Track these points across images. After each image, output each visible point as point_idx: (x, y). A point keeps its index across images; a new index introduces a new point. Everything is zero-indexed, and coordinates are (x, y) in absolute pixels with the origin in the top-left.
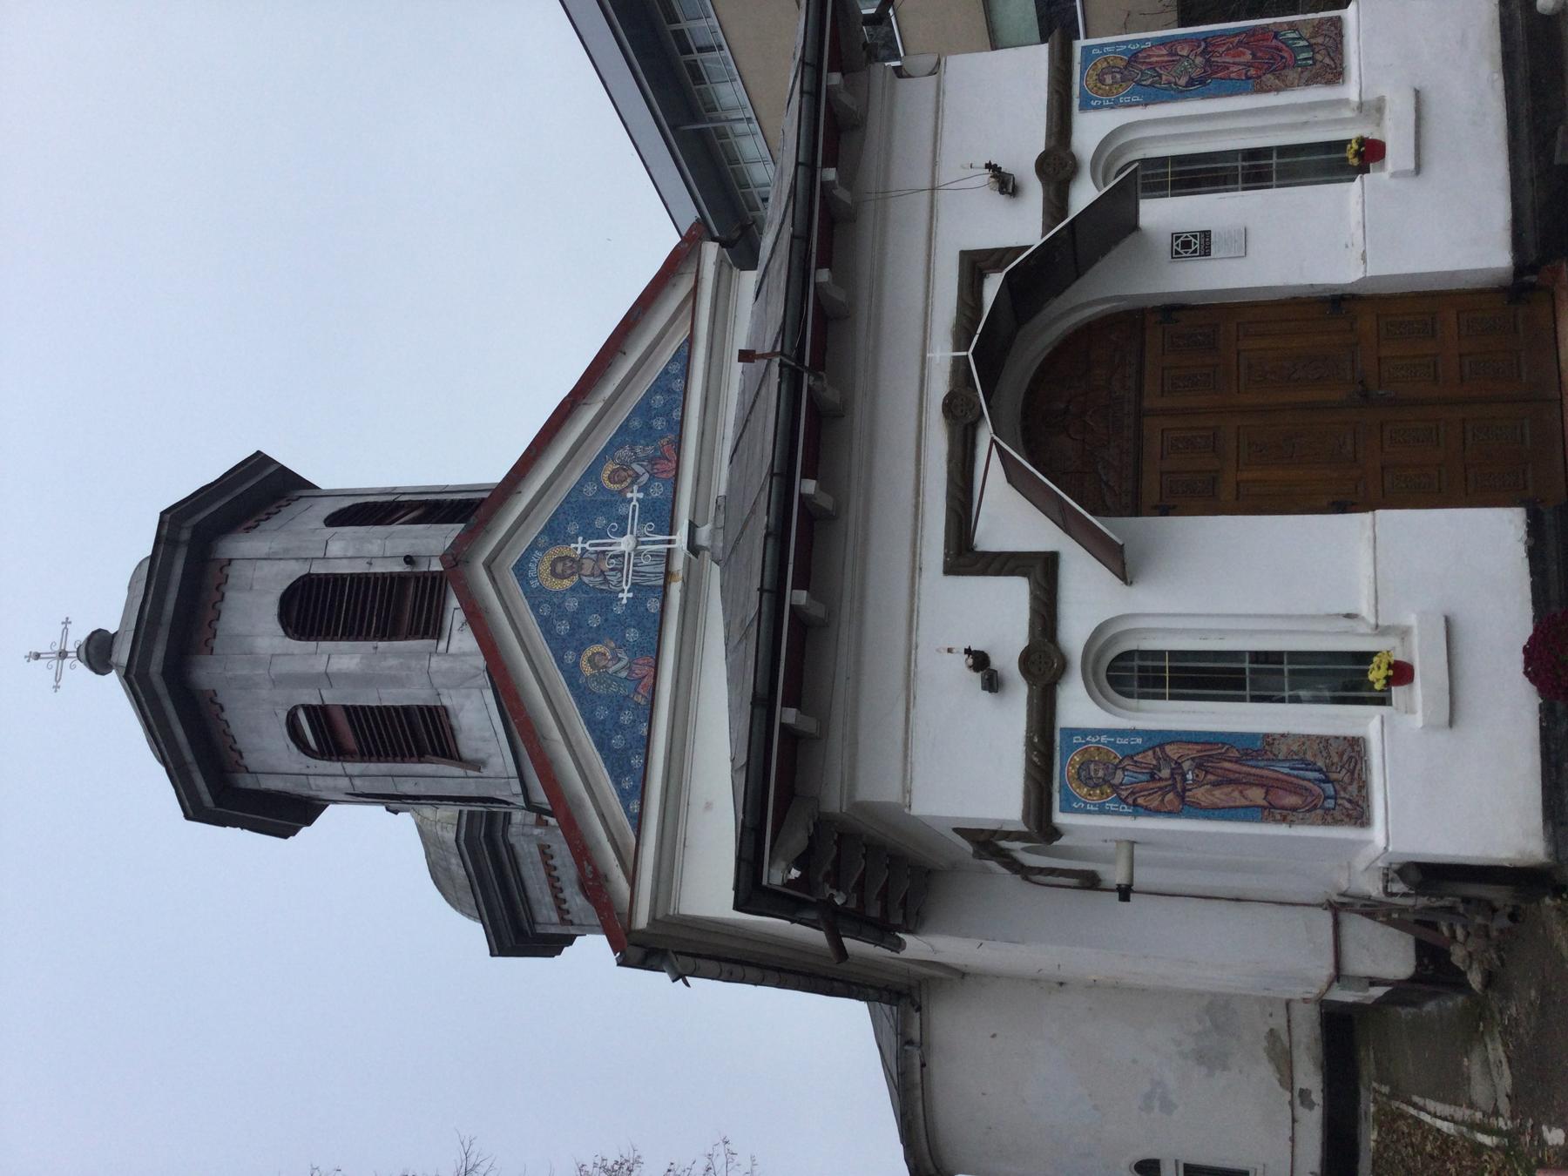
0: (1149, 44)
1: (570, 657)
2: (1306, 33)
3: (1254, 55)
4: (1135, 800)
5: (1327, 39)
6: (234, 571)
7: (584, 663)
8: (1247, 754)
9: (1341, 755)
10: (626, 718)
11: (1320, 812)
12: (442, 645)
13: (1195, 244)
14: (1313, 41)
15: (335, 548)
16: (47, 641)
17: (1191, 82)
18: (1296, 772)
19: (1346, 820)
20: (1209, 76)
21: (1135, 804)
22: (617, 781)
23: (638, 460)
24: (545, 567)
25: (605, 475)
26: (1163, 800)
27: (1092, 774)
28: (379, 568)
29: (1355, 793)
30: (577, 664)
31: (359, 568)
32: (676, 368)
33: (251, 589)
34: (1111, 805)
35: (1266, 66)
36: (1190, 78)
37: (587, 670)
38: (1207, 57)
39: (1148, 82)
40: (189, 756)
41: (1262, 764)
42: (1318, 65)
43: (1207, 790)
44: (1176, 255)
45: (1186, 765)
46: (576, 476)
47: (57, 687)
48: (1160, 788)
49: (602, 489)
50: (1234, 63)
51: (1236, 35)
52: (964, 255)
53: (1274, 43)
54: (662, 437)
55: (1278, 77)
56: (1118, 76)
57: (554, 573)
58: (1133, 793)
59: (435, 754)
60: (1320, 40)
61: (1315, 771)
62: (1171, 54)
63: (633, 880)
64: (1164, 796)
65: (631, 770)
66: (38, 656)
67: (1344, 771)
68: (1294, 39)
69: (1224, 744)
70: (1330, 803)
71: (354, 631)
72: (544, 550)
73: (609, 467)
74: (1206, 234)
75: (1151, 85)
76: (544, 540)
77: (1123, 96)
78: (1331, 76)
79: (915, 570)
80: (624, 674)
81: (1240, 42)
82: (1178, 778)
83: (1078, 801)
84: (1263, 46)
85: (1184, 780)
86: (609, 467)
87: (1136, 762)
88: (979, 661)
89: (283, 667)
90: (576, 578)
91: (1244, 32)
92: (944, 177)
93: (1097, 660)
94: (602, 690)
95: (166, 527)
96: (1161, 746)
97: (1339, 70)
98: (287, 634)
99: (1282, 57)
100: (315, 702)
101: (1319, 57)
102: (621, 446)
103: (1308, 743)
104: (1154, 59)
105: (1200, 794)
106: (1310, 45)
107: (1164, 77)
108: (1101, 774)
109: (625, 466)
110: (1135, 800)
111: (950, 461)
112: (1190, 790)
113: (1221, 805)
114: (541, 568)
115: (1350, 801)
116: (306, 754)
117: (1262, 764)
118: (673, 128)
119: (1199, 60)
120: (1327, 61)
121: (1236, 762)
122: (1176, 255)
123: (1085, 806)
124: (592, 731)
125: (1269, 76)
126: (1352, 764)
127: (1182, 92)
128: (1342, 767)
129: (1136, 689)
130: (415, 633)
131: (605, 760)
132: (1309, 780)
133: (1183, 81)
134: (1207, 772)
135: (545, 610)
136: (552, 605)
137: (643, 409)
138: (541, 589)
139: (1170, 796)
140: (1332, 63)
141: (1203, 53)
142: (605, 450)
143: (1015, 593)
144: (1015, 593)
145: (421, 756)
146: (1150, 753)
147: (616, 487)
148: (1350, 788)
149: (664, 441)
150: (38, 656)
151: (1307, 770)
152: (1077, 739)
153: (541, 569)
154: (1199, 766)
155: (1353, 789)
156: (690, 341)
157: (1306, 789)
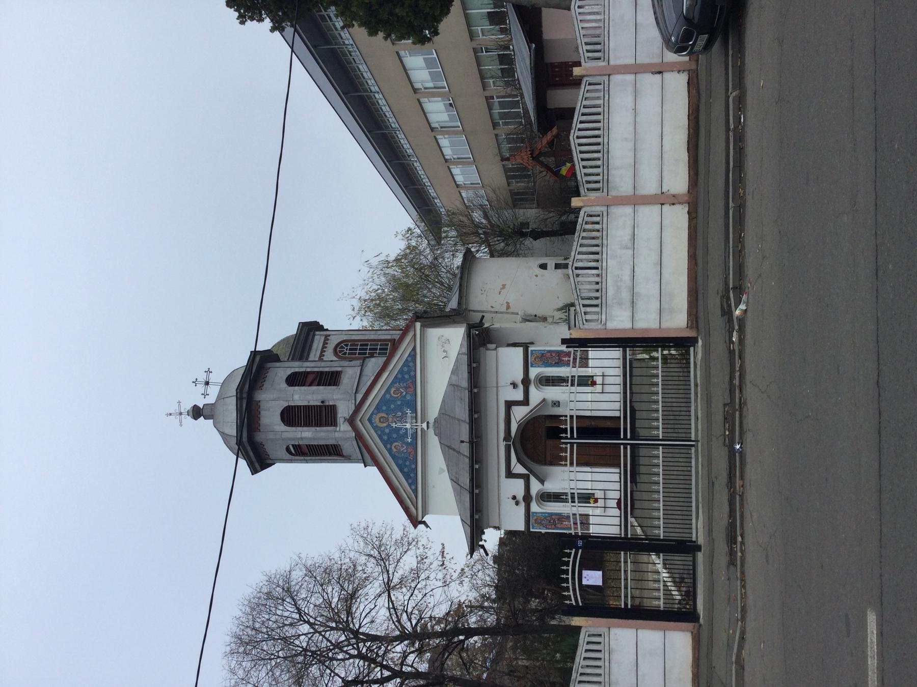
1: (389, 446)
6: (262, 404)
7: (393, 448)
10: (408, 463)
12: (338, 429)
15: (296, 397)
16: (174, 408)
17: (555, 363)
21: (546, 527)
22: (407, 480)
23: (402, 388)
24: (377, 420)
25: (392, 392)
28: (312, 403)
30: (391, 448)
31: (305, 403)
32: (409, 359)
33: (269, 411)
37: (395, 450)
40: (254, 459)
44: (553, 406)
45: (556, 520)
46: (383, 392)
47: (181, 425)
49: (391, 396)
52: (506, 402)
54: (408, 381)
57: (380, 421)
59: (335, 454)
63: (417, 509)
65: (411, 478)
66: (170, 414)
71: (308, 424)
72: (376, 414)
73: (393, 390)
75: (547, 363)
76: (375, 411)
79: (499, 477)
80: (405, 451)
86: (393, 390)
88: (514, 498)
89: (285, 435)
90: (387, 423)
92: (499, 385)
93: (538, 495)
94: (399, 455)
95: (239, 394)
96: (551, 516)
98: (285, 425)
100: (297, 443)
102: (396, 383)
105: (558, 525)
109: (397, 389)
111: (505, 452)
114: (376, 420)
116: (291, 455)
118: (314, 47)
122: (553, 406)
124: (398, 467)
129: (546, 499)
130: (327, 425)
131: (403, 475)
133: (554, 363)
135: (379, 433)
136: (381, 431)
137: (401, 371)
138: (377, 426)
142: (391, 384)
143: (521, 483)
144: (521, 483)
145: (330, 454)
147: (396, 396)
149: (409, 382)
150: (170, 414)
152: (535, 514)
153: (376, 419)
156: (414, 349)
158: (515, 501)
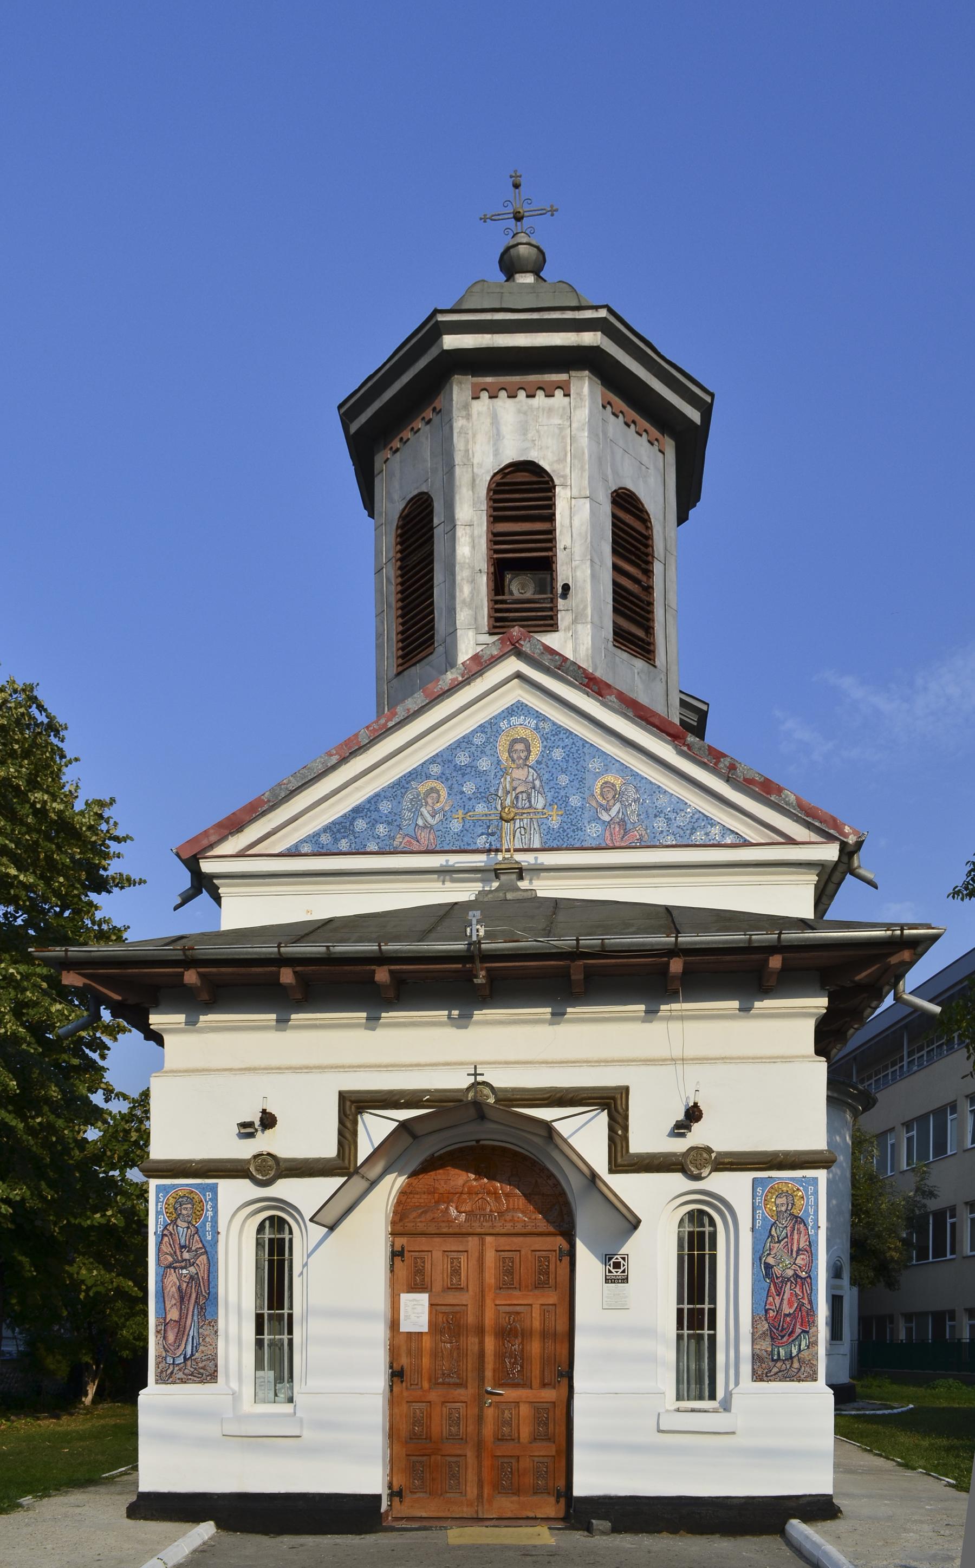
0: (811, 1232)
2: (805, 1354)
3: (789, 1315)
4: (166, 1235)
5: (796, 1371)
8: (202, 1308)
9: (203, 1368)
11: (164, 1354)
13: (617, 1272)
14: (795, 1360)
17: (768, 1267)
18: (190, 1339)
19: (159, 1370)
20: (773, 1281)
26: (168, 1254)
27: (184, 1206)
29: (178, 1376)
34: (162, 1219)
35: (777, 1325)
36: (772, 1267)
38: (792, 1279)
39: (773, 1232)
41: (195, 1318)
42: (771, 1364)
43: (175, 1284)
45: (192, 1270)
48: (175, 1252)
50: (782, 1299)
51: (810, 1302)
53: (798, 1331)
55: (764, 1333)
56: (783, 1209)
58: (171, 1234)
60: (796, 1365)
61: (192, 1352)
62: (799, 1250)
64: (171, 1255)
67: (192, 1370)
68: (800, 1345)
69: (209, 1294)
70: (170, 1360)
74: (625, 1280)
75: (770, 1235)
77: (763, 1213)
78: (760, 1373)
81: (803, 1304)
82: (183, 1264)
83: (164, 1197)
84: (795, 1322)
85: (182, 1268)
87: (194, 1236)
91: (812, 1307)
97: (765, 1379)
99: (783, 1337)
101: (779, 1364)
103: (211, 1347)
104: (796, 1237)
106: (791, 1358)
107: (777, 1245)
108: (184, 1212)
110: (166, 1235)
112: (175, 1272)
113: (165, 1291)
115: (172, 1373)
117: (195, 1318)
119: (790, 1273)
120: (775, 1370)
121: (196, 1302)
123: (160, 1202)
125: (766, 1326)
126: (197, 1375)
127: (760, 1259)
128: (195, 1369)
132: (185, 1348)
133: (771, 1261)
134: (188, 1283)
139: (170, 1259)
140: (772, 1373)
141: (796, 1276)
146: (200, 1245)
148: (181, 1373)
151: (192, 1347)
152: (209, 1195)
154: (192, 1278)
155: (180, 1375)
157: (179, 1346)
158: (257, 1123)
